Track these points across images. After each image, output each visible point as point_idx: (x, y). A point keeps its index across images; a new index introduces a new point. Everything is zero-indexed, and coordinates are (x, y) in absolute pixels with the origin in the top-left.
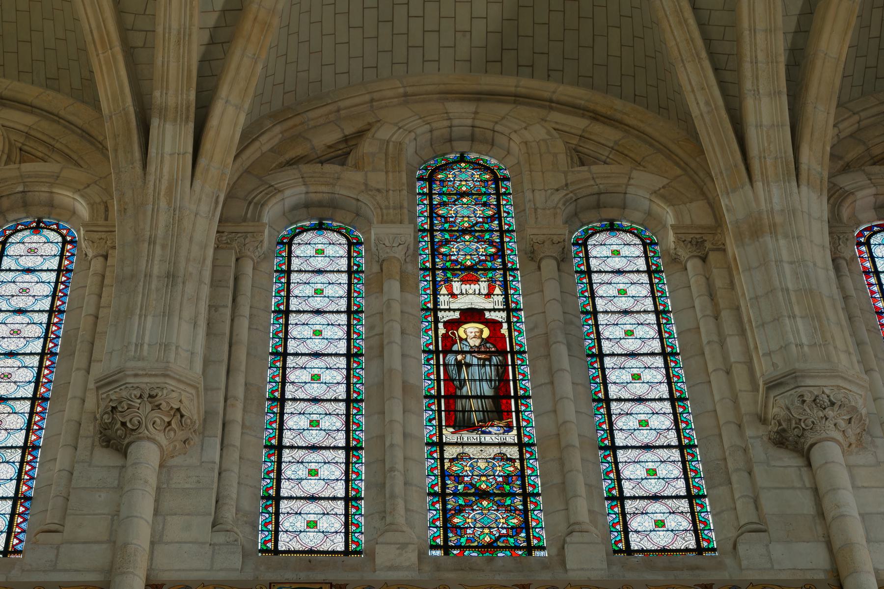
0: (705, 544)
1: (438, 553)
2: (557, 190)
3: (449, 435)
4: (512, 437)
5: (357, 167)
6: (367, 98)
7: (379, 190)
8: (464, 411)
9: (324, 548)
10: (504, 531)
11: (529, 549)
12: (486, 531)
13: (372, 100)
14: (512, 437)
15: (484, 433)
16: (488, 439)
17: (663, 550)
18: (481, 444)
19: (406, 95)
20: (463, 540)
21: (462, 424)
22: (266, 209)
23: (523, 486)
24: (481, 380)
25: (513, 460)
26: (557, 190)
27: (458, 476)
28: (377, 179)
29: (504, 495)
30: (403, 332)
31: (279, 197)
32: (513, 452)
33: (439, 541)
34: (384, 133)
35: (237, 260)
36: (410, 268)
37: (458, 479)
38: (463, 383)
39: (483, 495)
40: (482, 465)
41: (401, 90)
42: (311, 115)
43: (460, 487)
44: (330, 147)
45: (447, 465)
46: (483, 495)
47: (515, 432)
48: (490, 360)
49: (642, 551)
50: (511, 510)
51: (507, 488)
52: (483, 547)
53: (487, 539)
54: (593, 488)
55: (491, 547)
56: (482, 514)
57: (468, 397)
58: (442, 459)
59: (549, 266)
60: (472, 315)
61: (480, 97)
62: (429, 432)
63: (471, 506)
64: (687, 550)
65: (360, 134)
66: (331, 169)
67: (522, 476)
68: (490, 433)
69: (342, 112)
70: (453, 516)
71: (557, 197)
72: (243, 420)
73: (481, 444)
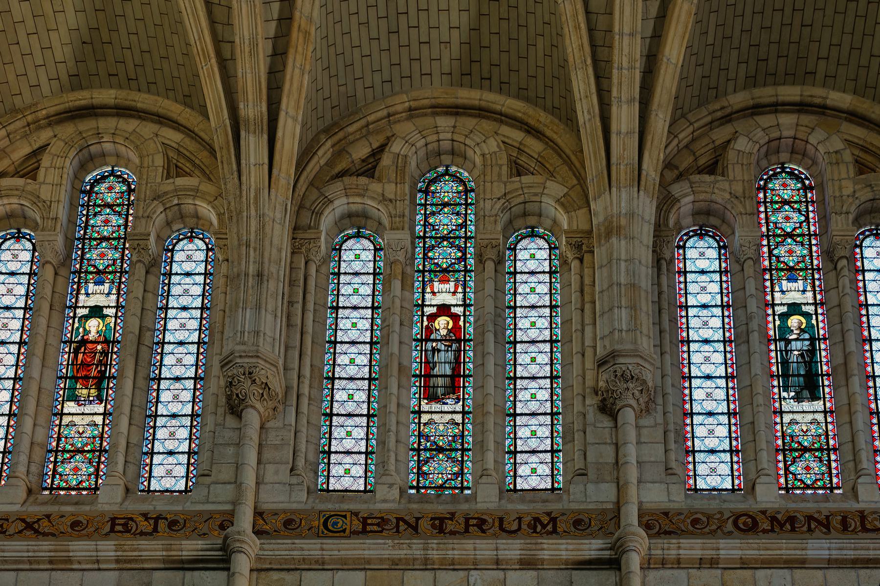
0: (556, 485)
1: (413, 491)
2: (499, 199)
3: (425, 407)
4: (459, 407)
5: (380, 180)
6: (384, 113)
7: (391, 201)
8: (434, 387)
9: (353, 488)
10: (449, 476)
11: (462, 488)
12: (440, 476)
13: (389, 115)
14: (459, 407)
15: (444, 403)
16: (446, 408)
17: (534, 490)
18: (442, 412)
19: (410, 109)
20: (427, 482)
21: (433, 398)
22: (323, 218)
23: (462, 444)
24: (445, 363)
25: (458, 424)
26: (499, 199)
27: (428, 436)
28: (390, 190)
29: (452, 450)
30: (401, 324)
31: (330, 208)
32: (458, 418)
33: (415, 483)
34: (396, 147)
35: (306, 263)
36: (408, 270)
37: (427, 438)
38: (435, 364)
39: (440, 450)
40: (441, 427)
41: (407, 104)
42: (351, 129)
43: (428, 444)
44: (363, 161)
45: (422, 428)
46: (440, 450)
47: (461, 403)
48: (451, 346)
49: (522, 490)
50: (453, 460)
51: (454, 444)
52: (438, 487)
53: (440, 482)
54: (499, 444)
55: (442, 487)
56: (438, 464)
57: (437, 376)
58: (419, 423)
59: (490, 265)
60: (444, 310)
61: (457, 110)
62: (414, 402)
63: (433, 458)
64: (546, 490)
65: (382, 148)
66: (363, 180)
67: (463, 436)
68: (447, 404)
69: (370, 127)
70: (423, 465)
71: (498, 206)
72: (310, 393)
73: (442, 412)
